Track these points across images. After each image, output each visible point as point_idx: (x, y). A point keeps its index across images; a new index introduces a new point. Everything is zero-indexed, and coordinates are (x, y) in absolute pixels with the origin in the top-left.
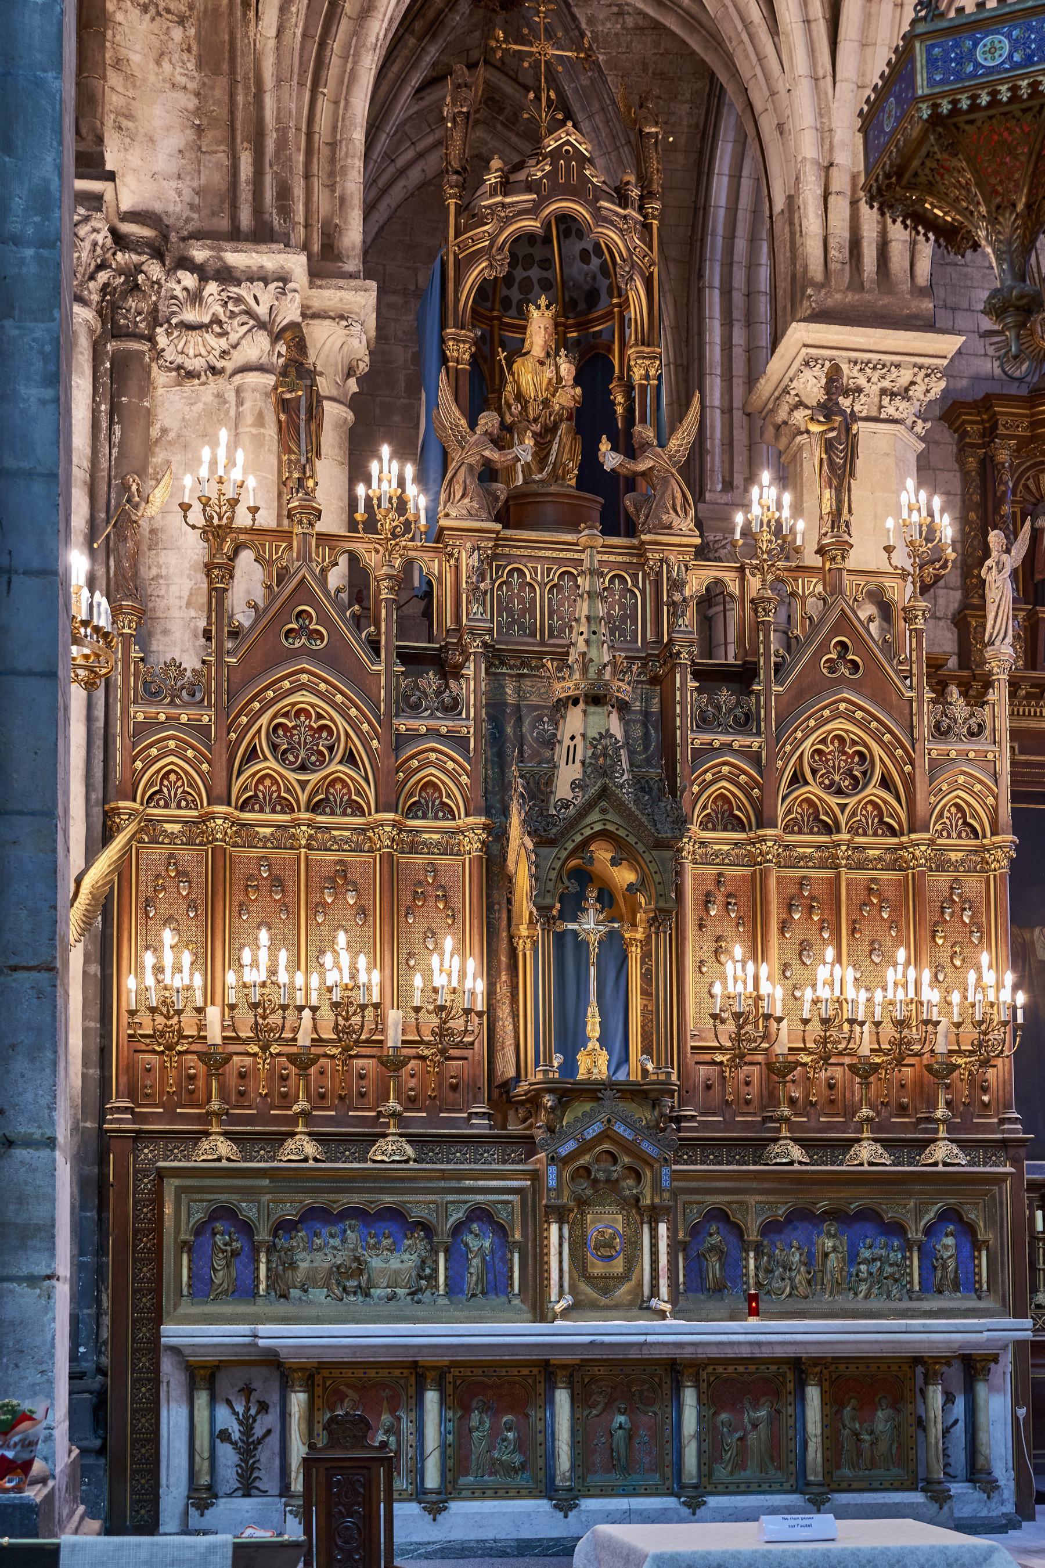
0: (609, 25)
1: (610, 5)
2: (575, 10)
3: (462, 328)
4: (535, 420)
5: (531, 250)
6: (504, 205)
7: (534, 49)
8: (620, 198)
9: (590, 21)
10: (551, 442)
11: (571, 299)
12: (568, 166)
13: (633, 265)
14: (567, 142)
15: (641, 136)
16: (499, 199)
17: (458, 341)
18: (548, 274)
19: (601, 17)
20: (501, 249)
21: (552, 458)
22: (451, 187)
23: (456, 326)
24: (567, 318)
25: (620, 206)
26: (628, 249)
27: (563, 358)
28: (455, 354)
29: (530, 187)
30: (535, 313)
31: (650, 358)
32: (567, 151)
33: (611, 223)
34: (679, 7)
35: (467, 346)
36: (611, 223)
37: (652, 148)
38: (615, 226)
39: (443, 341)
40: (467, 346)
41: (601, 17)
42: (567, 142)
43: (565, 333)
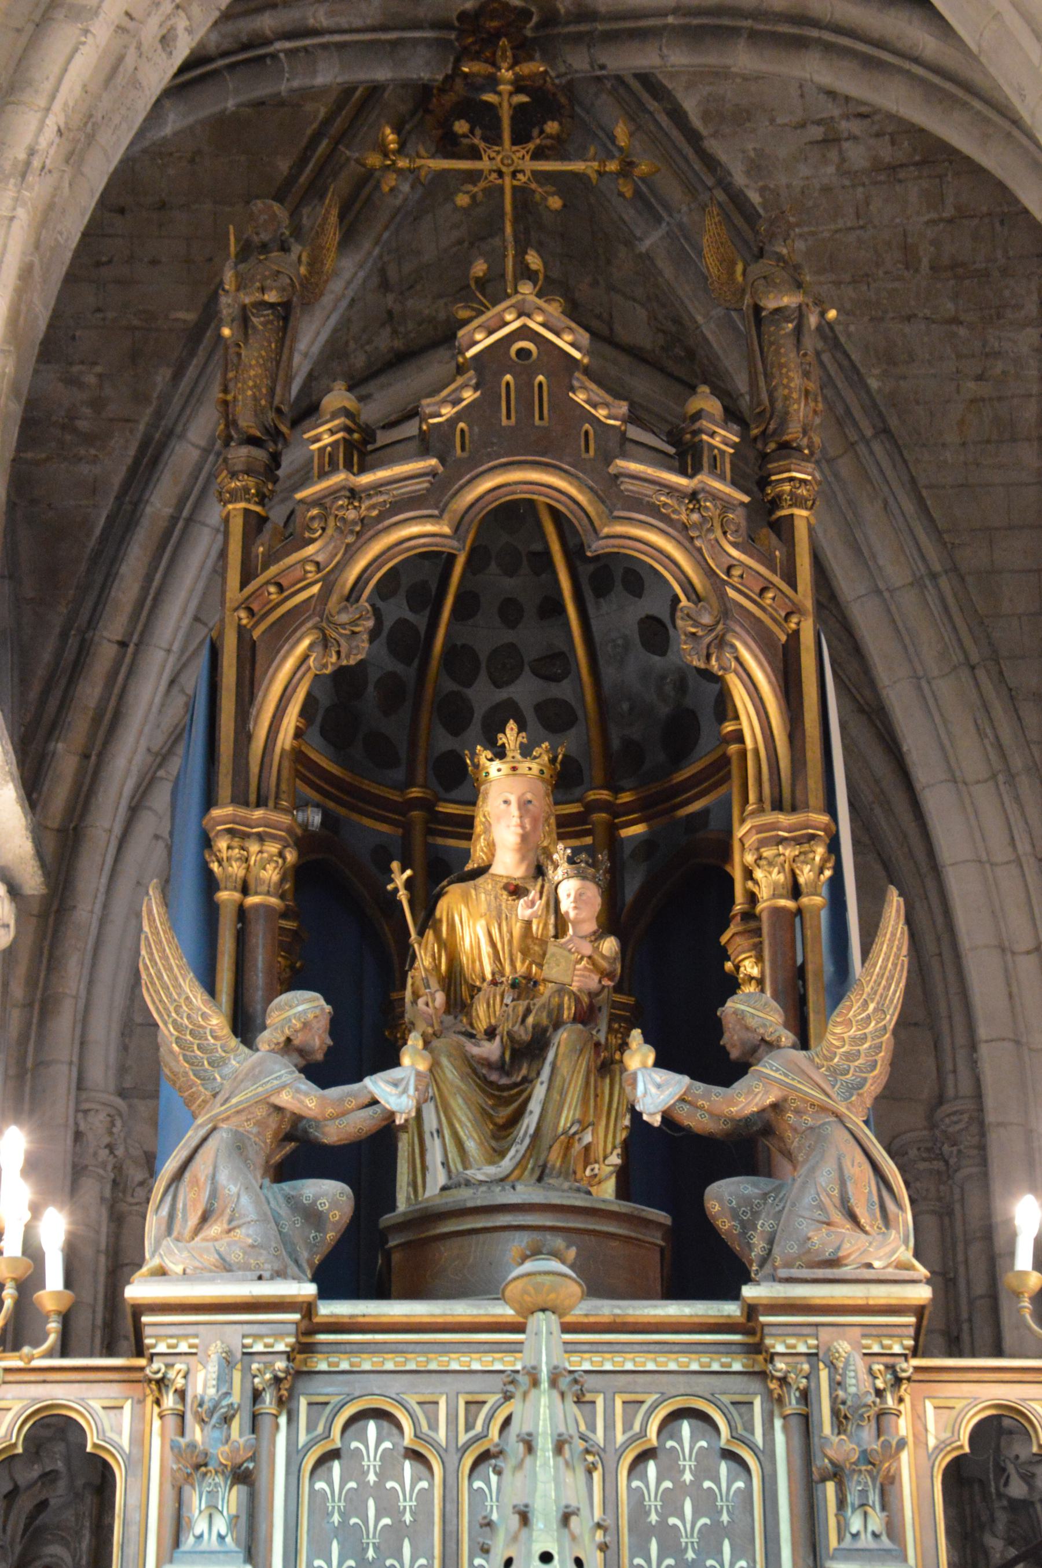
0: (804, 170)
1: (802, 125)
2: (714, 146)
3: (260, 803)
4: (491, 1033)
5: (508, 636)
6: (353, 494)
7: (484, 165)
8: (681, 455)
9: (756, 167)
10: (528, 1081)
11: (628, 744)
12: (525, 384)
13: (726, 611)
14: (524, 333)
15: (759, 321)
16: (340, 478)
17: (245, 836)
18: (563, 690)
19: (782, 153)
20: (353, 596)
21: (530, 1122)
22: (233, 475)
23: (240, 799)
24: (616, 790)
25: (683, 472)
26: (710, 573)
27: (564, 868)
28: (236, 869)
29: (424, 445)
30: (495, 770)
31: (798, 841)
32: (523, 353)
33: (654, 510)
34: (917, 60)
35: (273, 848)
36: (654, 510)
37: (789, 343)
38: (666, 519)
39: (206, 842)
40: (273, 848)
41: (782, 153)
42: (524, 333)
43: (612, 829)
